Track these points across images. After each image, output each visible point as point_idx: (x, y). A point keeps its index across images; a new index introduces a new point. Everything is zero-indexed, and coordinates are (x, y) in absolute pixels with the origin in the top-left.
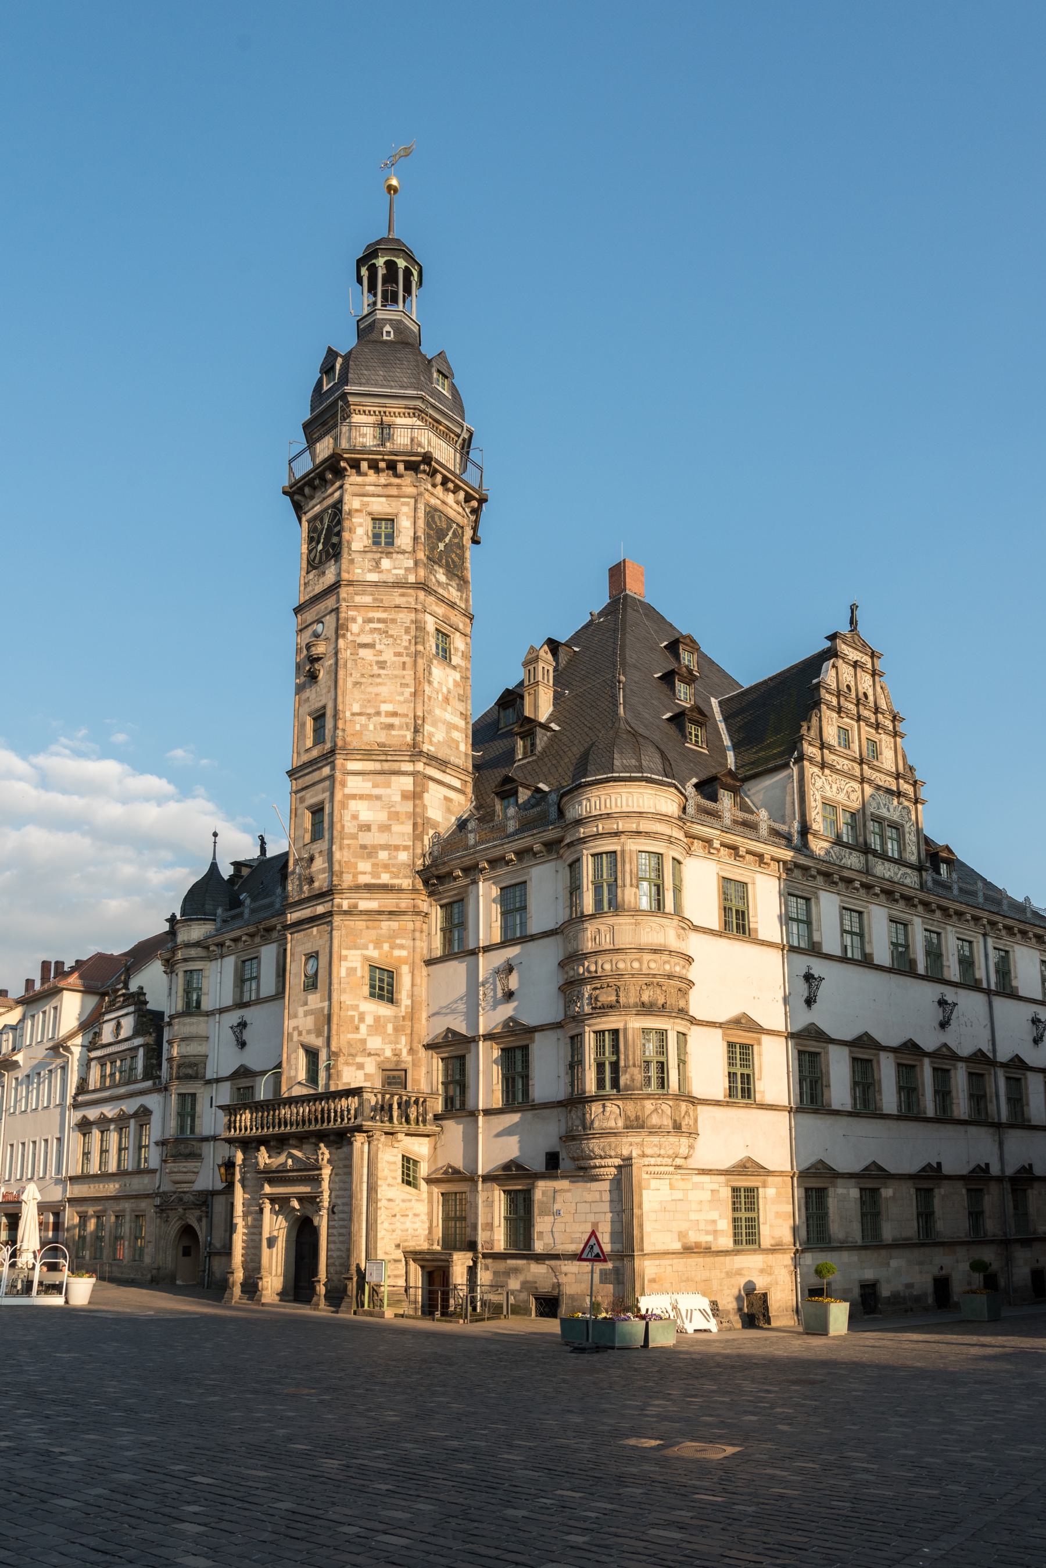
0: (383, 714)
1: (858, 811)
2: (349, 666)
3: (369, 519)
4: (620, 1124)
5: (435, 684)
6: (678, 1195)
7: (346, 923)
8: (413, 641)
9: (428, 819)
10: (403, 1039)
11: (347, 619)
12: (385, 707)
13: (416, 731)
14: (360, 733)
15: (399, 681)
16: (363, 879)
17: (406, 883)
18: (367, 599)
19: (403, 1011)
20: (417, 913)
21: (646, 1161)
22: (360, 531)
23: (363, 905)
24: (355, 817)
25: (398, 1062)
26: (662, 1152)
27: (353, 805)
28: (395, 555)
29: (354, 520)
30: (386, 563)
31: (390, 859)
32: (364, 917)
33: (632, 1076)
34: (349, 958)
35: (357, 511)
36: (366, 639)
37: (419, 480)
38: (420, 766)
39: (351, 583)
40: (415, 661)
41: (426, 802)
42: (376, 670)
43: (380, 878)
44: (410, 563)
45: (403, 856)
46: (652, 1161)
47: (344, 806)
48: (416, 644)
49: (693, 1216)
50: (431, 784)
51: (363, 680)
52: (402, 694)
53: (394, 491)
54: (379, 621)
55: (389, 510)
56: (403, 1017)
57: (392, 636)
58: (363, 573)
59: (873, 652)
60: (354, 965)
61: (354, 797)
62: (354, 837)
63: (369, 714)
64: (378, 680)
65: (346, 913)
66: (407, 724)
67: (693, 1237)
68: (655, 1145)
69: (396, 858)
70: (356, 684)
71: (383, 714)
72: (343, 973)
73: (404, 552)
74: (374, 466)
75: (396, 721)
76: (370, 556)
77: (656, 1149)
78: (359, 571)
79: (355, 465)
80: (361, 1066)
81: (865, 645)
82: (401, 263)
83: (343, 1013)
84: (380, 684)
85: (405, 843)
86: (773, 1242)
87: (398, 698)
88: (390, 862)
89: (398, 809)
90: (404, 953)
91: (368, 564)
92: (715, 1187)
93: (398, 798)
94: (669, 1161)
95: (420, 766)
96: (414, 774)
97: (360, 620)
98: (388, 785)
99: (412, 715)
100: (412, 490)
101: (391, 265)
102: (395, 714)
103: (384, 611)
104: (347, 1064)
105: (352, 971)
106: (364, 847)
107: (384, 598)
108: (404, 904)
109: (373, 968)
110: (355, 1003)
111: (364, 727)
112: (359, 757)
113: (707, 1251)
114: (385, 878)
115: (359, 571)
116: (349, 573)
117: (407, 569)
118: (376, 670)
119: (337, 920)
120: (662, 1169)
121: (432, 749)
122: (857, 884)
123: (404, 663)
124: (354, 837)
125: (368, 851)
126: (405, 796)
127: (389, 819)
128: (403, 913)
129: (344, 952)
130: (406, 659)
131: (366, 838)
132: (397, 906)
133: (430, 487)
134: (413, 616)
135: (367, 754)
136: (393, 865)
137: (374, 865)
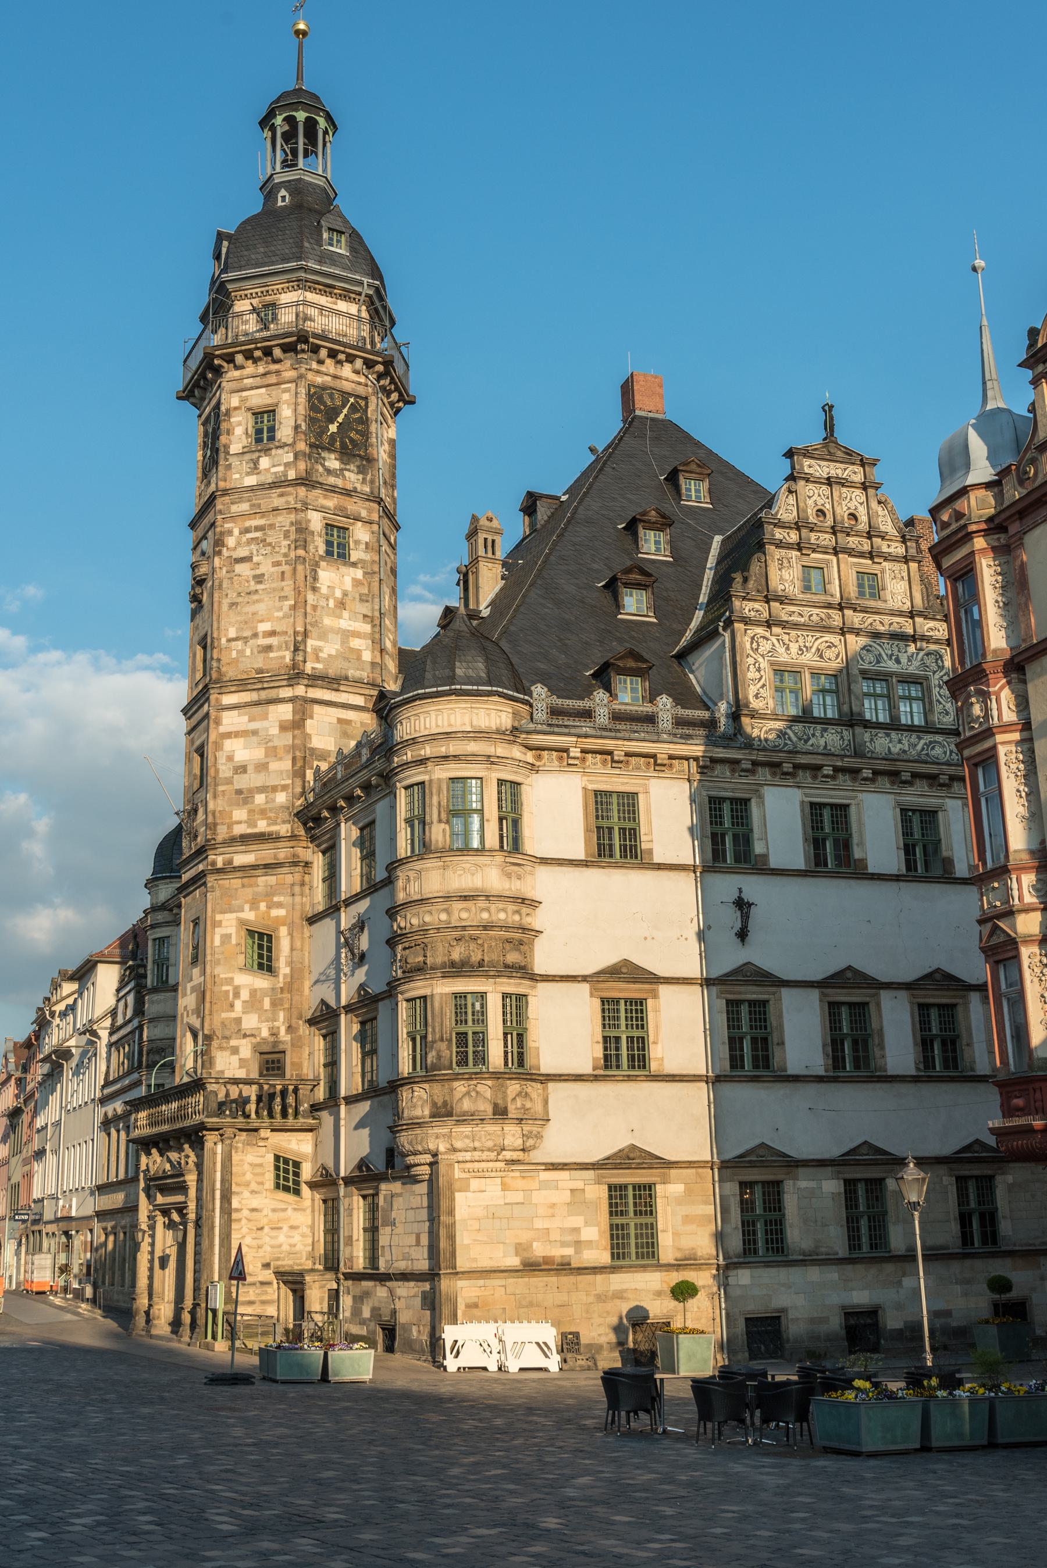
0: (261, 635)
1: (841, 671)
2: (224, 586)
3: (249, 414)
4: (427, 1112)
5: (324, 590)
6: (518, 1197)
8: (293, 546)
9: (313, 750)
10: (281, 1015)
11: (222, 533)
12: (264, 627)
13: (296, 649)
14: (236, 661)
15: (278, 594)
17: (284, 829)
18: (244, 507)
19: (281, 981)
20: (295, 864)
21: (460, 1156)
22: (239, 431)
23: (239, 860)
24: (230, 758)
25: (276, 1043)
26: (477, 1144)
27: (229, 745)
28: (273, 452)
29: (232, 420)
30: (264, 462)
31: (267, 802)
33: (439, 1051)
34: (224, 924)
35: (236, 408)
36: (242, 552)
37: (299, 362)
38: (300, 690)
39: (225, 492)
40: (295, 569)
41: (308, 730)
42: (253, 585)
43: (256, 826)
44: (290, 457)
45: (281, 798)
46: (468, 1156)
47: (218, 746)
48: (296, 548)
49: (539, 1224)
50: (317, 708)
51: (240, 599)
52: (281, 608)
53: (273, 379)
54: (258, 529)
55: (269, 401)
56: (281, 988)
57: (270, 544)
58: (242, 478)
59: (862, 460)
60: (229, 931)
61: (228, 735)
62: (229, 781)
64: (256, 597)
65: (219, 871)
66: (286, 643)
67: (539, 1250)
68: (467, 1137)
69: (273, 800)
70: (233, 605)
71: (261, 635)
72: (217, 942)
74: (249, 355)
75: (274, 641)
76: (248, 457)
77: (467, 1141)
78: (237, 476)
79: (230, 359)
80: (235, 1051)
81: (849, 453)
82: (301, 116)
83: (216, 989)
84: (257, 601)
85: (283, 782)
86: (679, 1255)
87: (276, 614)
89: (276, 742)
90: (282, 912)
91: (245, 467)
92: (579, 1185)
93: (275, 731)
94: (493, 1155)
95: (300, 690)
96: (291, 700)
97: (236, 532)
98: (265, 717)
99: (291, 632)
100: (292, 374)
101: (291, 120)
102: (273, 633)
103: (262, 517)
104: (221, 1048)
105: (226, 938)
106: (239, 792)
107: (261, 502)
108: (283, 853)
109: (251, 933)
111: (241, 653)
112: (233, 689)
113: (564, 1267)
114: (262, 826)
115: (237, 476)
116: (225, 481)
119: (210, 879)
120: (484, 1165)
121: (319, 666)
122: (828, 771)
123: (283, 573)
124: (229, 781)
125: (243, 797)
126: (283, 727)
127: (266, 756)
129: (218, 917)
130: (286, 568)
131: (242, 782)
132: (276, 858)
133: (314, 365)
134: (292, 517)
135: (242, 685)
136: (271, 810)
137: (251, 812)
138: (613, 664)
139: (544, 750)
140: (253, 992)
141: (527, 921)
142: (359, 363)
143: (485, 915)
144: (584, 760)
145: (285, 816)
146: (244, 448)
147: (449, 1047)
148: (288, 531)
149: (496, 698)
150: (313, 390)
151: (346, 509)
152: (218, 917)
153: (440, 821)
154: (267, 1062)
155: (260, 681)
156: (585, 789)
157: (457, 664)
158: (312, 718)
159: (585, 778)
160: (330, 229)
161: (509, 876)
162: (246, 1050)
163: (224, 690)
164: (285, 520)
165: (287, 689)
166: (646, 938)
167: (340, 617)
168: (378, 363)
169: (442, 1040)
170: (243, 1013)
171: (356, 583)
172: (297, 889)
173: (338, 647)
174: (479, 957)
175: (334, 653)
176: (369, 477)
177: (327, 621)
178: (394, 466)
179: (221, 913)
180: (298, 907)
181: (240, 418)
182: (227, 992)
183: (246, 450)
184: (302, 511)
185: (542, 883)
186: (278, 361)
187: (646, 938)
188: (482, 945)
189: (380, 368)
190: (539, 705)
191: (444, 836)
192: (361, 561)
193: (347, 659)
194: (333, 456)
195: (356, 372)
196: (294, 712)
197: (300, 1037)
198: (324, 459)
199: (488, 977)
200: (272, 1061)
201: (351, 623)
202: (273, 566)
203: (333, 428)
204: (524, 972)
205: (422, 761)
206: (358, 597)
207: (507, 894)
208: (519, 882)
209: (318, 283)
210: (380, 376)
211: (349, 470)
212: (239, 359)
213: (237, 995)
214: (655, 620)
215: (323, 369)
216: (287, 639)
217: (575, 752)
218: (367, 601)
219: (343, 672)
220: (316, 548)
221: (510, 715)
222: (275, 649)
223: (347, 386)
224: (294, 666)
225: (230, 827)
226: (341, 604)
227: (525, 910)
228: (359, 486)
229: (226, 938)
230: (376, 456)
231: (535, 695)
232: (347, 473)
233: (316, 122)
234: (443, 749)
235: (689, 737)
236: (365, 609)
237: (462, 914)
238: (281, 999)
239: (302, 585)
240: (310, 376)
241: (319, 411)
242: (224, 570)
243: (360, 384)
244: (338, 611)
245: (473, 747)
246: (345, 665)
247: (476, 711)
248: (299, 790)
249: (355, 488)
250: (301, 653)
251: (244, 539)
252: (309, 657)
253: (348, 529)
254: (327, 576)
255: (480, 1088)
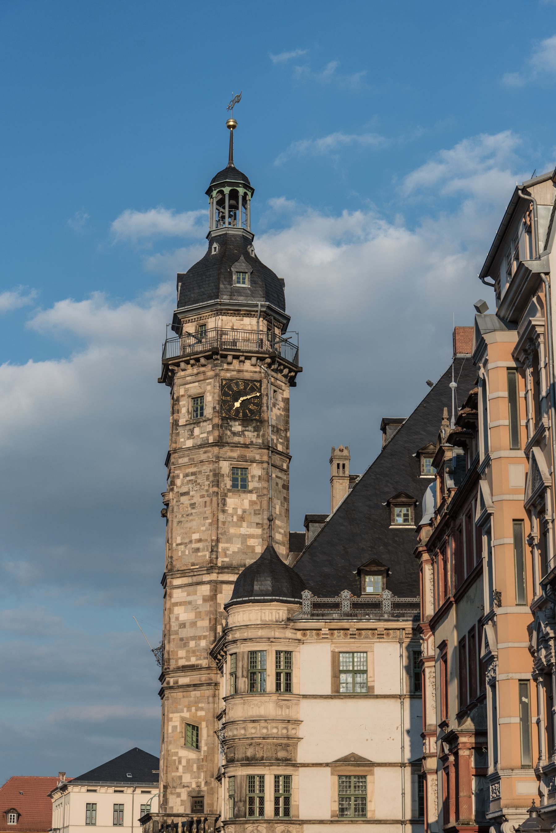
0: (194, 541)
2: (175, 510)
3: (190, 399)
5: (230, 511)
7: (172, 694)
8: (211, 485)
10: (202, 775)
11: (174, 477)
12: (195, 536)
13: (212, 551)
16: (182, 663)
17: (204, 663)
20: (209, 684)
22: (184, 410)
23: (184, 680)
24: (177, 619)
25: (199, 791)
28: (202, 424)
29: (180, 403)
30: (197, 431)
31: (196, 646)
32: (181, 690)
33: (239, 808)
34: (174, 719)
35: (182, 396)
36: (184, 489)
38: (213, 577)
40: (211, 500)
42: (190, 510)
43: (190, 661)
44: (210, 428)
51: (183, 519)
52: (204, 525)
53: (201, 377)
54: (193, 474)
55: (200, 391)
56: (202, 759)
57: (199, 484)
58: (185, 441)
61: (176, 604)
62: (177, 633)
63: (186, 543)
64: (191, 518)
65: (171, 688)
66: (207, 546)
69: (199, 645)
70: (180, 522)
73: (209, 420)
76: (188, 427)
78: (182, 440)
80: (179, 795)
83: (169, 758)
84: (192, 520)
85: (204, 634)
88: (196, 648)
89: (201, 609)
90: (202, 713)
91: (187, 434)
93: (200, 602)
96: (209, 582)
97: (181, 476)
99: (209, 540)
102: (200, 541)
103: (195, 466)
104: (172, 793)
105: (175, 728)
106: (182, 639)
108: (203, 677)
110: (176, 750)
111: (183, 552)
112: (178, 576)
114: (193, 661)
116: (176, 443)
117: (208, 433)
118: (190, 510)
121: (227, 560)
123: (206, 502)
124: (177, 633)
125: (184, 642)
126: (205, 600)
128: (201, 685)
129: (171, 715)
130: (207, 499)
132: (200, 681)
133: (225, 366)
134: (211, 466)
135: (183, 573)
137: (188, 652)
138: (363, 569)
139: (307, 630)
140: (188, 761)
141: (292, 733)
142: (254, 360)
143: (265, 731)
144: (332, 634)
145: (205, 654)
146: (186, 421)
147: (245, 805)
148: (208, 475)
149: (275, 603)
150: (224, 382)
151: (246, 456)
152: (171, 715)
153: (243, 676)
154: (196, 802)
155: (192, 570)
156: (333, 652)
157: (255, 583)
158: (221, 593)
159: (334, 645)
160: (237, 272)
161: (281, 707)
162: (184, 796)
163: (174, 576)
164: (207, 468)
165: (207, 575)
166: (367, 740)
167: (241, 526)
168: (267, 358)
169: (241, 801)
170: (183, 773)
171: (252, 503)
172: (211, 699)
173: (239, 546)
174: (261, 755)
175: (236, 550)
176: (261, 433)
177: (232, 531)
178: (288, 416)
179: (172, 713)
180: (212, 710)
181: (184, 402)
182: (175, 760)
183: (187, 423)
184: (216, 462)
185: (305, 710)
186: (204, 366)
187: (367, 740)
188: (263, 748)
189: (268, 360)
190: (306, 603)
191: (245, 685)
192: (255, 488)
193: (245, 553)
194: (237, 423)
195: (254, 365)
196: (211, 591)
197: (212, 788)
198: (231, 426)
199: (265, 766)
200: (197, 802)
201: (248, 529)
202: (201, 498)
203: (237, 405)
204: (289, 762)
205: (235, 641)
206: (253, 512)
207: (280, 718)
208: (287, 710)
209: (230, 310)
210: (269, 366)
211: (248, 431)
212: (183, 365)
213: (180, 762)
214: (415, 527)
215: (231, 367)
216: (207, 544)
217: (325, 631)
218: (259, 514)
219: (243, 562)
220: (225, 484)
221: (286, 612)
222: (201, 550)
223: (247, 376)
224: (211, 561)
225: (177, 661)
226: (242, 519)
227: (290, 726)
228: (254, 440)
229: (175, 728)
230: (266, 419)
231: (304, 597)
232: (246, 433)
233: (237, 192)
234: (246, 634)
235: (403, 615)
236: (258, 519)
237: (252, 730)
238: (202, 765)
239: (215, 510)
240: (223, 374)
241: (229, 395)
242: (175, 501)
243: (255, 372)
244: (239, 523)
245: (260, 633)
246: (244, 557)
247: (264, 611)
248: (212, 639)
249: (252, 442)
250: (214, 553)
251: (185, 481)
252: (220, 555)
253: (247, 468)
254: (232, 502)
255: (259, 828)
